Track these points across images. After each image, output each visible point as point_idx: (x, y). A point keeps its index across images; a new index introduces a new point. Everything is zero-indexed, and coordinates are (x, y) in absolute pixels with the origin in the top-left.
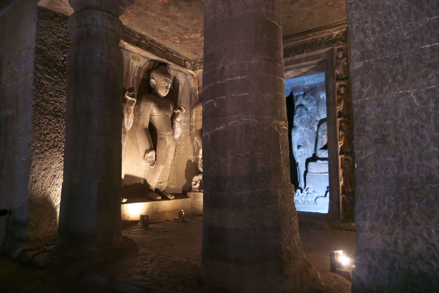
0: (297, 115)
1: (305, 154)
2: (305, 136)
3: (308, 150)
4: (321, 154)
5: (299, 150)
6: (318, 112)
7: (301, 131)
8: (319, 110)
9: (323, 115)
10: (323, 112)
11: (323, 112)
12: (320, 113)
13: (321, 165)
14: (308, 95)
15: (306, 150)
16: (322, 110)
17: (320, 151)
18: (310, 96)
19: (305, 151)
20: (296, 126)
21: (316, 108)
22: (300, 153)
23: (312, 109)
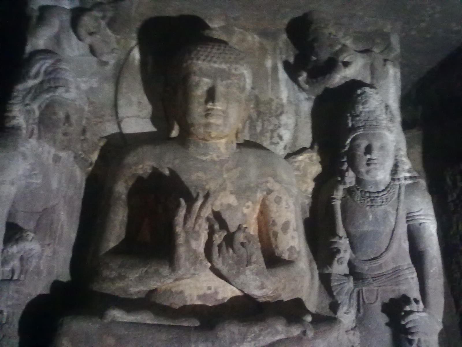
0: (31, 83)
1: (38, 272)
2: (55, 185)
3: (55, 252)
4: (121, 277)
5: (14, 249)
6: (115, 106)
7: (37, 156)
8: (121, 102)
9: (133, 120)
10: (133, 110)
11: (133, 110)
12: (123, 112)
13: (122, 331)
14: (96, 19)
15: (48, 251)
16: (130, 103)
17: (115, 263)
18: (103, 23)
19: (40, 257)
20: (17, 129)
21: (109, 88)
22: (16, 263)
23: (91, 89)
